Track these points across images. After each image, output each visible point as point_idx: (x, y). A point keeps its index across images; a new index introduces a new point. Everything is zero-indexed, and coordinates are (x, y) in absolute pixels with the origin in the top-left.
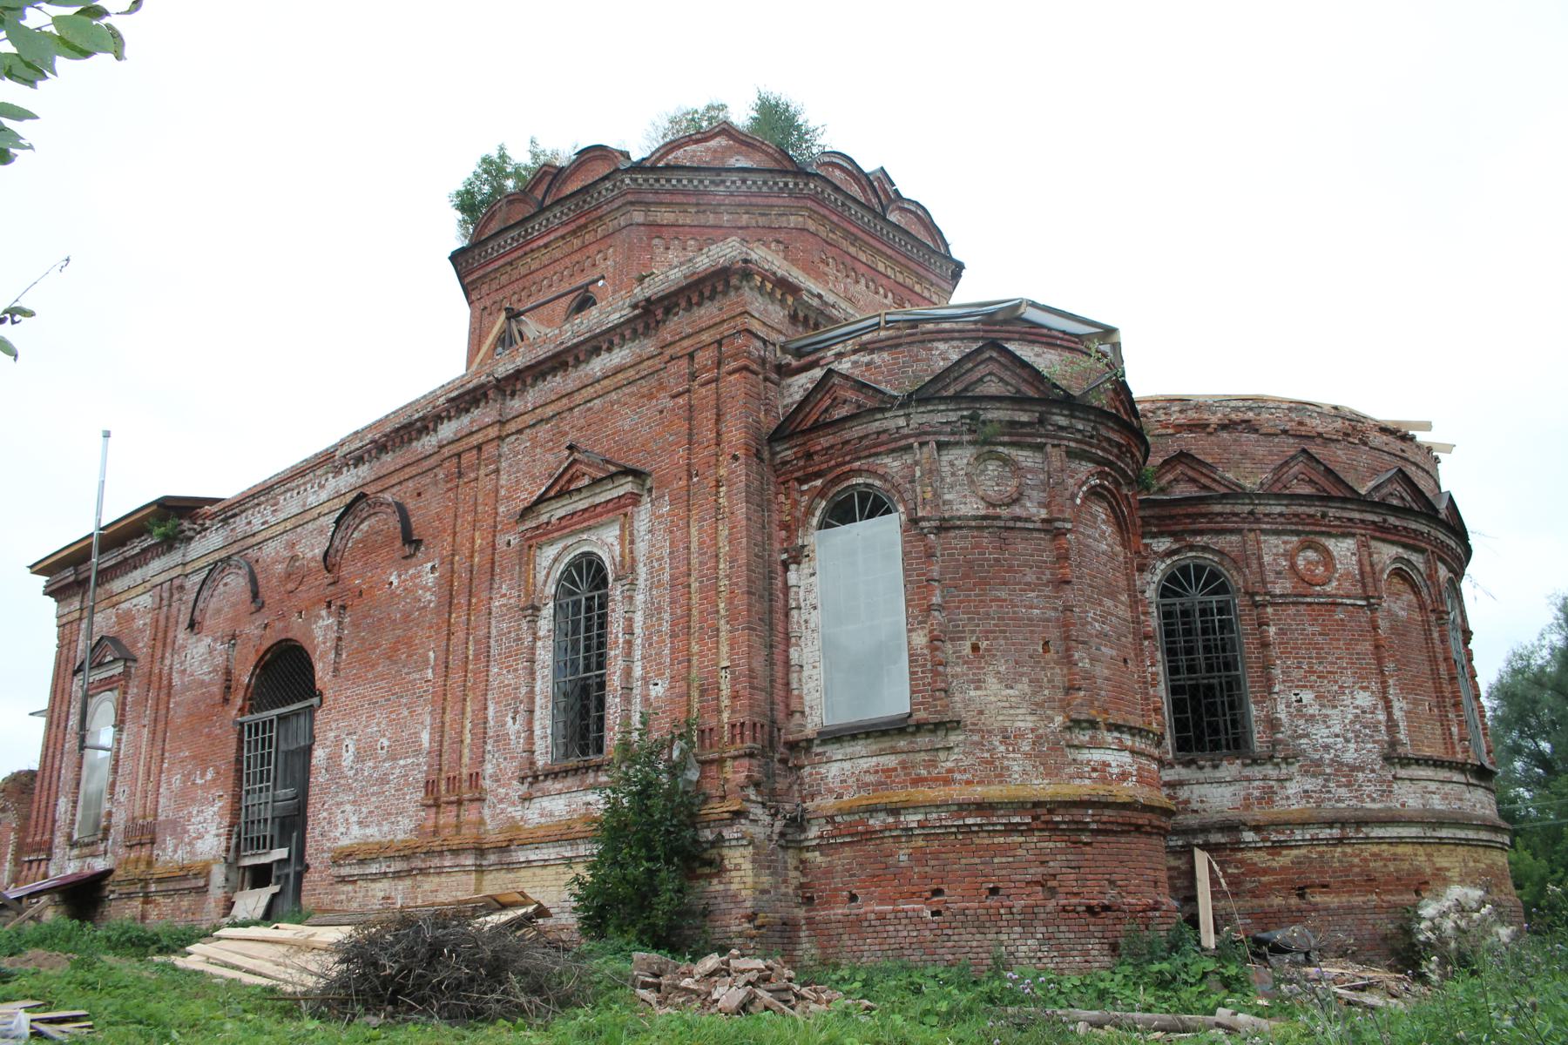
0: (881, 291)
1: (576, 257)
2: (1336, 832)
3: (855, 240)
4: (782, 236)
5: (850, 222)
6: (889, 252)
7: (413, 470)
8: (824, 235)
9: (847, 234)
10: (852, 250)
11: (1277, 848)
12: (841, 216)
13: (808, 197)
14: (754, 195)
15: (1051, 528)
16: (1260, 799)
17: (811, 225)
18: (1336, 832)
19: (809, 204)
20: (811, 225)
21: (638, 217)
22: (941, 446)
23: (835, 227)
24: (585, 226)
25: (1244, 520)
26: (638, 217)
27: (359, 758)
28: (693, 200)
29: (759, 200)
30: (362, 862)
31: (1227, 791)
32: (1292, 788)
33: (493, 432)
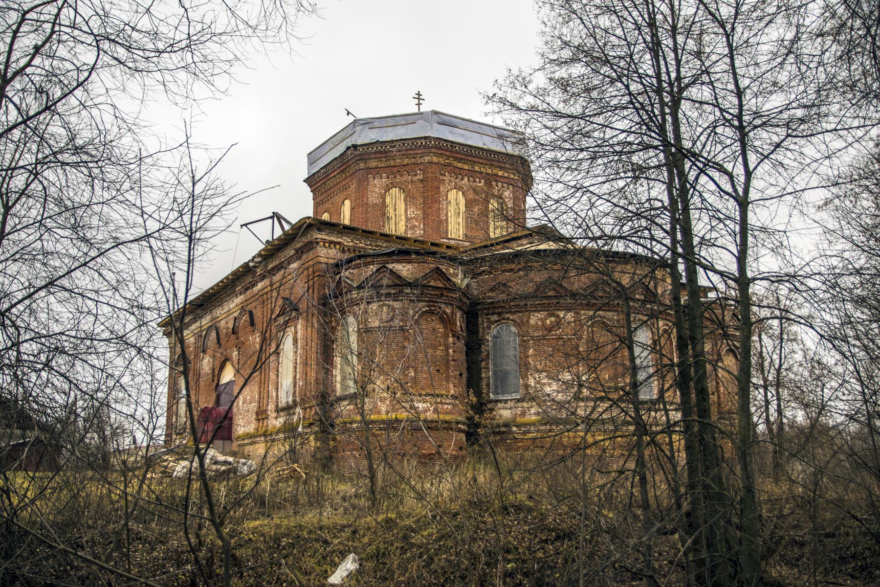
0: (478, 180)
1: (344, 183)
2: (548, 427)
3: (460, 160)
4: (422, 167)
5: (457, 153)
6: (481, 161)
7: (253, 299)
8: (443, 162)
9: (456, 159)
10: (459, 165)
11: (525, 433)
12: (451, 151)
13: (432, 147)
14: (409, 150)
15: (402, 329)
16: (520, 415)
17: (435, 159)
18: (548, 427)
19: (433, 150)
20: (435, 159)
21: (362, 166)
22: (368, 303)
23: (448, 157)
24: (345, 169)
25: (523, 307)
26: (362, 166)
27: (243, 403)
28: (384, 155)
29: (411, 152)
30: (243, 439)
31: (509, 412)
32: (533, 411)
33: (269, 288)
